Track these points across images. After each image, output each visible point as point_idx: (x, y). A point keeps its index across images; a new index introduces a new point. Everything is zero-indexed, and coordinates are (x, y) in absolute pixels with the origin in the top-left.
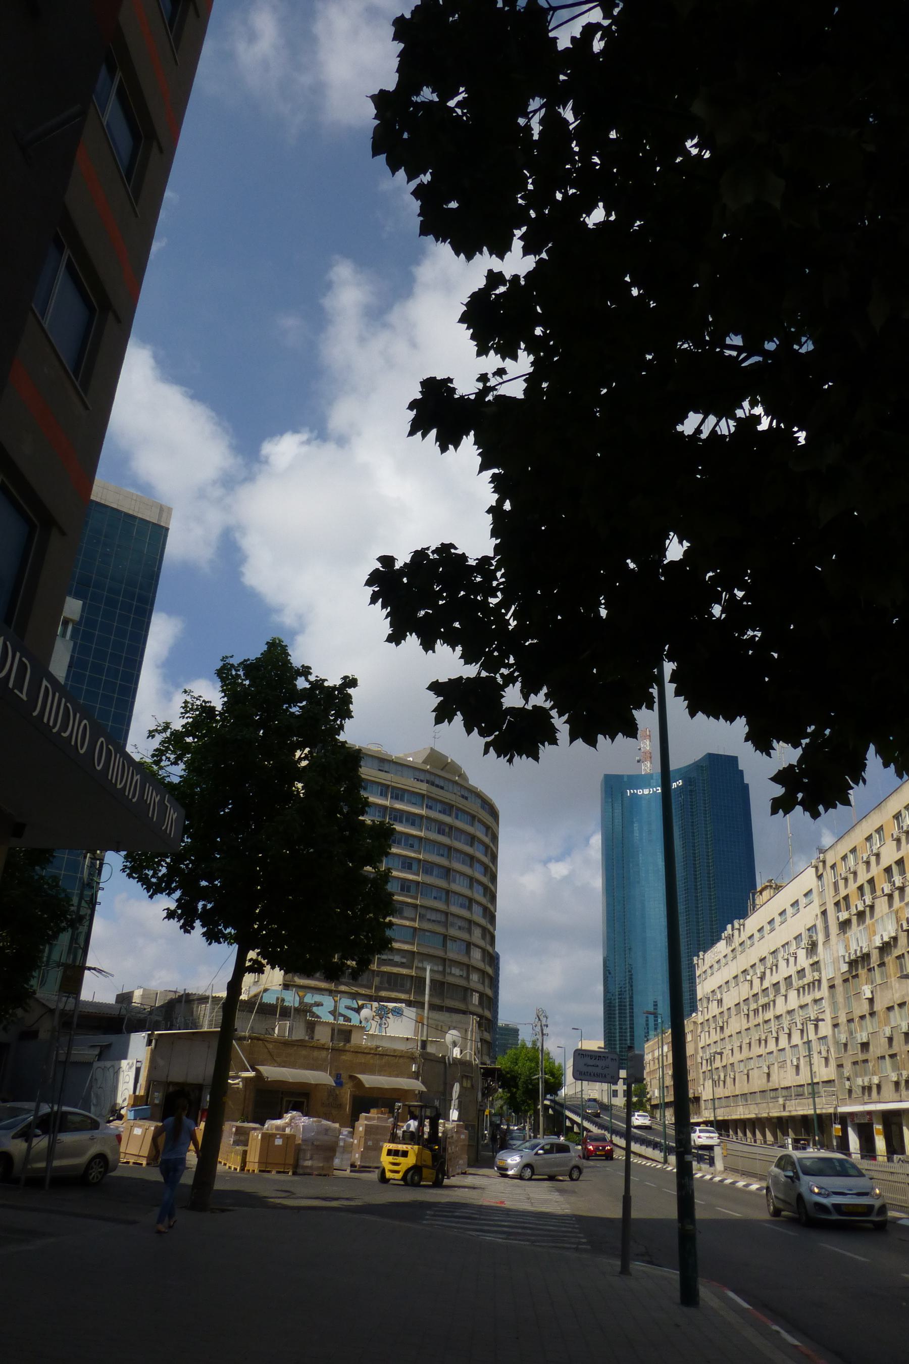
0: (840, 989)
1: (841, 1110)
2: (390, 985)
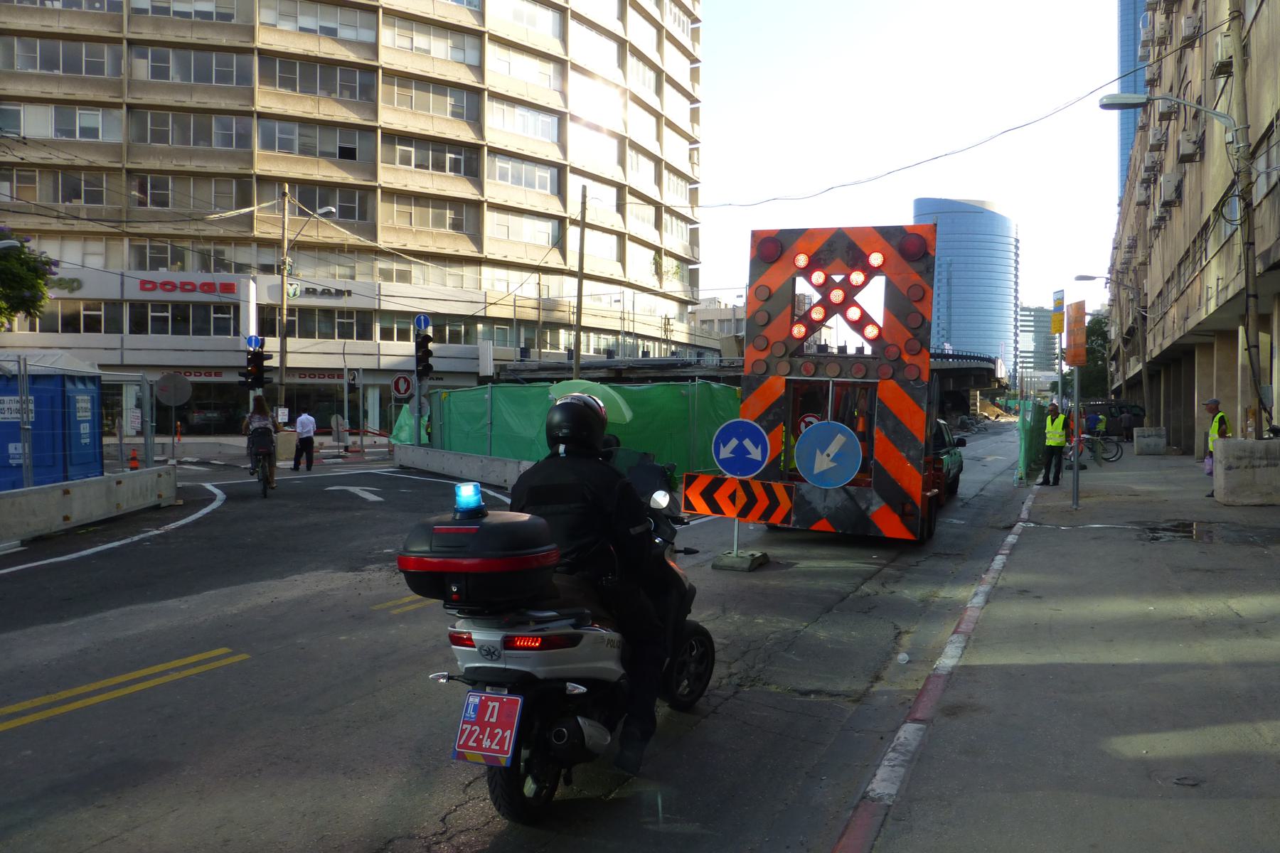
2: (186, 77)
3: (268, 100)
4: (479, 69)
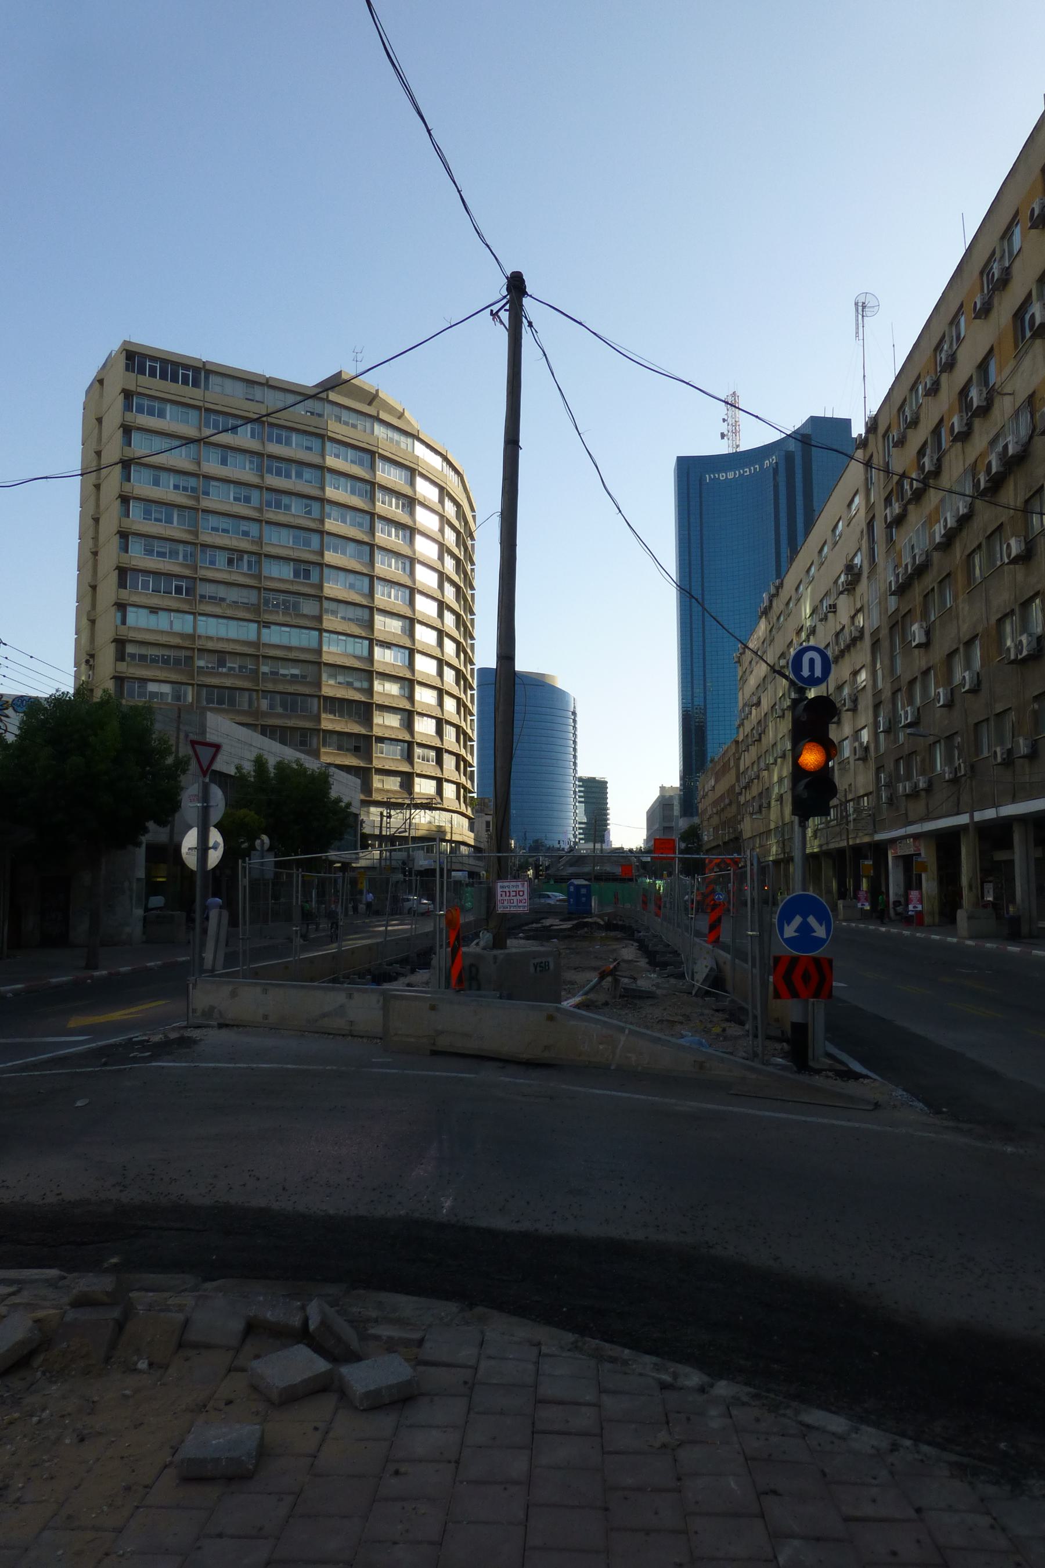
0: (885, 644)
1: (879, 837)
2: (286, 709)
3: (329, 722)
4: (411, 698)
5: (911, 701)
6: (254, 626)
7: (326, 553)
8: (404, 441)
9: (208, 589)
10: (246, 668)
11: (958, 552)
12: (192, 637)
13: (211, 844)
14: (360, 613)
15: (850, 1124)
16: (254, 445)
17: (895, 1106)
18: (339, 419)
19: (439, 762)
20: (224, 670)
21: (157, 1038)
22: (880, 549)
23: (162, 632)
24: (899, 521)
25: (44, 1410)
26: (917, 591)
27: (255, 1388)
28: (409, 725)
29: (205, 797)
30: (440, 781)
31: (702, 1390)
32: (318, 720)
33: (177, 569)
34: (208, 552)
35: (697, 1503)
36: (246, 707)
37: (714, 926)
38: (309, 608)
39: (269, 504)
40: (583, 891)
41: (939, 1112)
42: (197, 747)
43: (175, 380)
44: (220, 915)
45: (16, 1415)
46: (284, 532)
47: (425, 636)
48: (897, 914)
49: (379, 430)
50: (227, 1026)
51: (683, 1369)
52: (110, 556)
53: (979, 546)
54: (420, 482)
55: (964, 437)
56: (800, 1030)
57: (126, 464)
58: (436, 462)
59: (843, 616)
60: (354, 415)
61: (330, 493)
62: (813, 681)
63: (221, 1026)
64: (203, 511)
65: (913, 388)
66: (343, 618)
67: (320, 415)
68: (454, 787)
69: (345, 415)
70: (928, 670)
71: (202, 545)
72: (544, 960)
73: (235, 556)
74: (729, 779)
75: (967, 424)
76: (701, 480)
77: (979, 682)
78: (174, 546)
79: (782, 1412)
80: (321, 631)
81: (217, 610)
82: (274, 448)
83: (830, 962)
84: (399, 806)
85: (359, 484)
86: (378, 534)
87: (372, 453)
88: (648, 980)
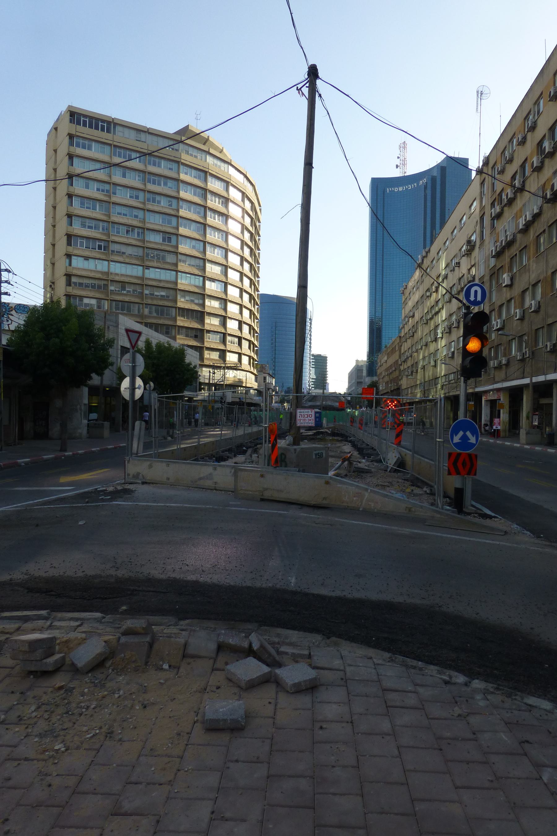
1: (477, 390)
2: (158, 314)
3: (181, 322)
4: (225, 309)
5: (500, 316)
6: (141, 268)
7: (180, 228)
8: (223, 166)
9: (116, 247)
10: (136, 291)
11: (532, 234)
12: (107, 273)
13: (137, 386)
14: (198, 262)
15: (494, 542)
16: (140, 166)
17: (515, 533)
18: (187, 153)
19: (240, 344)
20: (125, 292)
21: (111, 489)
22: (487, 232)
23: (91, 270)
24: (499, 216)
25: (119, 690)
26: (507, 255)
27: (230, 680)
28: (224, 324)
29: (134, 360)
30: (240, 355)
31: (466, 684)
32: (175, 320)
33: (98, 236)
34: (116, 226)
35: (488, 747)
36: (136, 312)
37: (399, 435)
38: (170, 258)
39: (149, 200)
40: (318, 415)
41: (539, 537)
42: (129, 333)
43: (97, 128)
44: (141, 424)
45: (106, 693)
46: (157, 216)
47: (233, 276)
48: (485, 431)
49: (210, 159)
50: (146, 483)
51: (454, 673)
52: (62, 227)
53: (544, 231)
54: (231, 189)
55: (539, 169)
56: (459, 492)
57: (70, 177)
58: (240, 178)
59: (464, 269)
60: (195, 150)
61: (183, 194)
62: (476, 303)
63: (143, 483)
64: (113, 203)
65: (511, 141)
66: (189, 265)
67: (177, 150)
68: (247, 358)
69: (191, 150)
70: (511, 299)
71: (112, 222)
72: (320, 452)
73: (130, 228)
74: (395, 357)
75: (541, 162)
76: (384, 192)
77: (539, 307)
78: (97, 222)
79: (514, 697)
80: (177, 271)
81: (121, 259)
82: (151, 169)
83: (476, 456)
84: (219, 368)
85: (198, 190)
86: (208, 218)
87: (206, 172)
88: (364, 464)
